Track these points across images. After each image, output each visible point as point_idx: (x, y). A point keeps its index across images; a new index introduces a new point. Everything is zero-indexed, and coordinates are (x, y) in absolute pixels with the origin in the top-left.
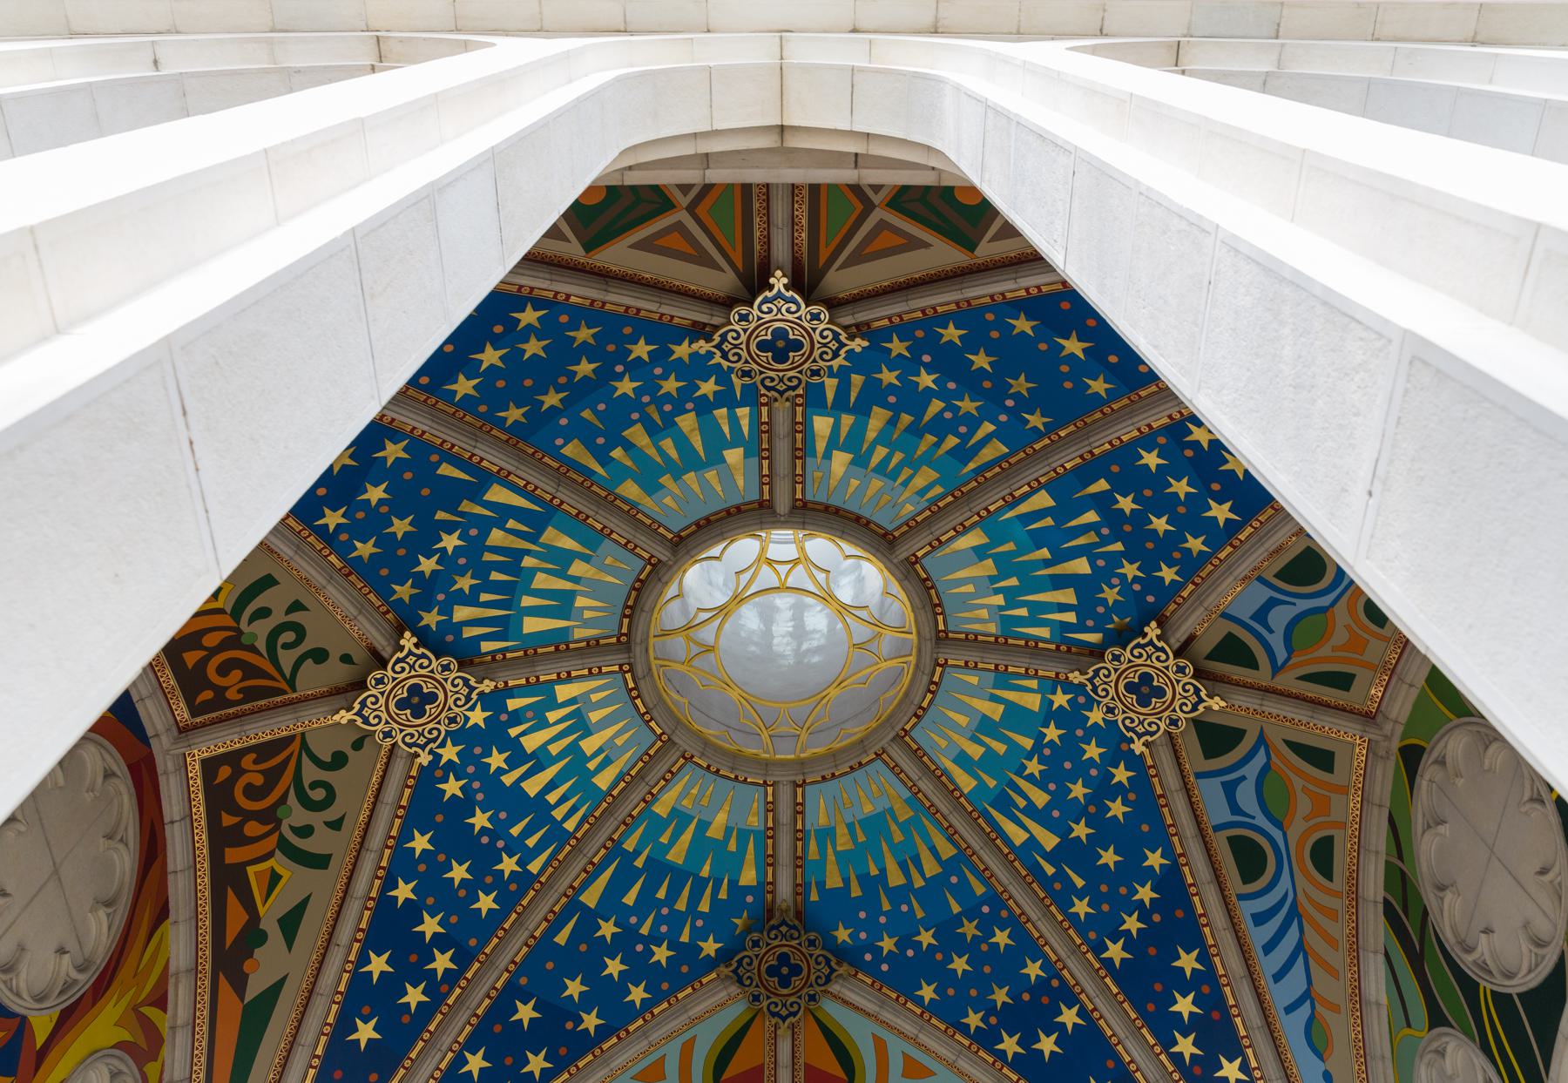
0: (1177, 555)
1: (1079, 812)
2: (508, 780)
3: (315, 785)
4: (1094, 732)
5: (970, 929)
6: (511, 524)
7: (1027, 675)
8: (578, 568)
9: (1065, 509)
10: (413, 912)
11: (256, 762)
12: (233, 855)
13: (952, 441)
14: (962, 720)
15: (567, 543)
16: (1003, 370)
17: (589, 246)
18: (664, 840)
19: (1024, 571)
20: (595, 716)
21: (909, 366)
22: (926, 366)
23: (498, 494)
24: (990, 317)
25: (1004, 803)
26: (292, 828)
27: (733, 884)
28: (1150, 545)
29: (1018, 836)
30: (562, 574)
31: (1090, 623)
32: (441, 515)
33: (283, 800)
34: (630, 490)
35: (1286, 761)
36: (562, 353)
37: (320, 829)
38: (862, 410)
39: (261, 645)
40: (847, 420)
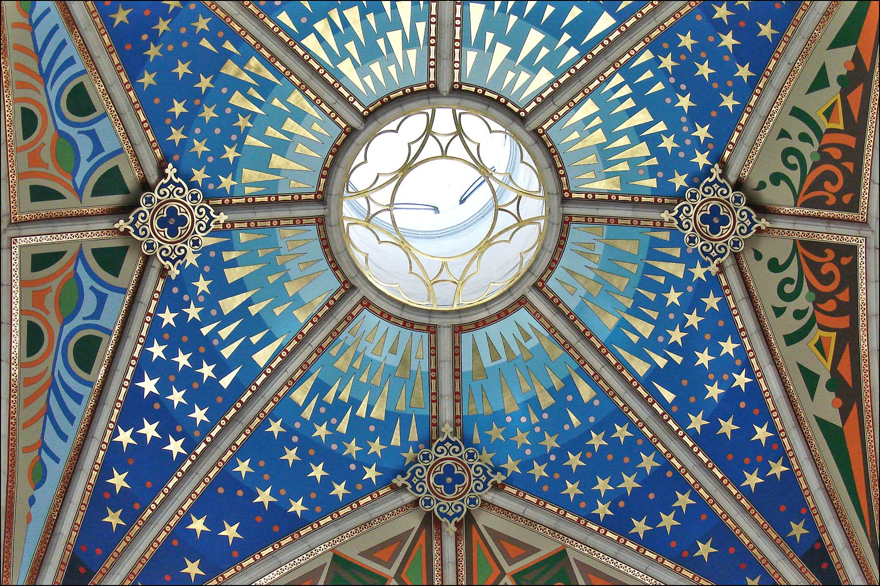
1: (206, 97)
2: (661, 127)
3: (793, 167)
4: (200, 162)
6: (635, 338)
9: (246, 352)
11: (827, 198)
12: (850, 141)
13: (330, 397)
14: (301, 149)
16: (303, 466)
17: (561, 555)
18: (544, 51)
21: (364, 460)
22: (353, 461)
23: (641, 368)
24: (318, 509)
25: (265, 87)
28: (185, 339)
29: (254, 62)
31: (212, 254)
32: (678, 359)
33: (815, 165)
35: (66, 186)
36: (586, 478)
38: (391, 416)
39: (805, 289)
40: (401, 406)
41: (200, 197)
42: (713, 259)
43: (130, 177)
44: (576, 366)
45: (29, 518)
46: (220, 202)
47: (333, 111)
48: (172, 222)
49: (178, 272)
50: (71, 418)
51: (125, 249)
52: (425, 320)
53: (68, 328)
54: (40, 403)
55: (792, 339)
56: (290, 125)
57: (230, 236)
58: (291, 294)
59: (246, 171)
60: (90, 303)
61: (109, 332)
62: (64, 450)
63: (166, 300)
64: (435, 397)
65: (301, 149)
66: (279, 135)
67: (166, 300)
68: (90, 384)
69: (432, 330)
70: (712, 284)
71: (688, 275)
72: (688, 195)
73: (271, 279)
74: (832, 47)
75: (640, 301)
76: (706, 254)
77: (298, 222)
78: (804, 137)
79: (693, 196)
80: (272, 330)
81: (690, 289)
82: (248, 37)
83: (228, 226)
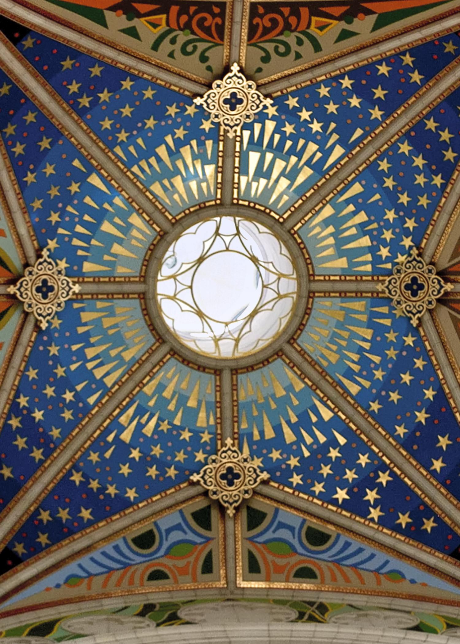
0: (309, 481)
3: (195, 48)
5: (69, 396)
6: (319, 155)
7: (216, 418)
8: (284, 183)
9: (322, 425)
10: (115, 88)
11: (217, 24)
14: (184, 385)
15: (300, 179)
19: (282, 411)
20: (193, 185)
23: (338, 151)
26: (177, 35)
27: (85, 258)
28: (311, 468)
30: (283, 174)
32: (333, 125)
33: (193, 33)
34: (328, 211)
35: (205, 547)
37: (171, 47)
39: (281, 38)
41: (214, 457)
42: (261, 102)
43: (200, 504)
44: (338, 195)
45: (424, 585)
46: (219, 442)
47: (158, 364)
48: (230, 476)
49: (265, 473)
50: (360, 550)
51: (248, 508)
52: (304, 300)
53: (300, 550)
54: (350, 572)
55: (317, 48)
56: (167, 394)
57: (243, 435)
58: (284, 393)
59: (198, 424)
60: (284, 534)
61: (304, 521)
62: (381, 557)
63: (285, 481)
64: (359, 295)
65: (184, 385)
66: (174, 401)
67: (285, 481)
68: (338, 536)
69: (311, 295)
70: (280, 102)
71: (273, 118)
72: (216, 120)
73: (273, 406)
74: (105, 26)
75: (292, 151)
76: (258, 107)
77: (234, 388)
78: (173, 41)
79: (217, 116)
80: (308, 406)
81: (283, 117)
82: (105, 425)
83: (236, 436)
